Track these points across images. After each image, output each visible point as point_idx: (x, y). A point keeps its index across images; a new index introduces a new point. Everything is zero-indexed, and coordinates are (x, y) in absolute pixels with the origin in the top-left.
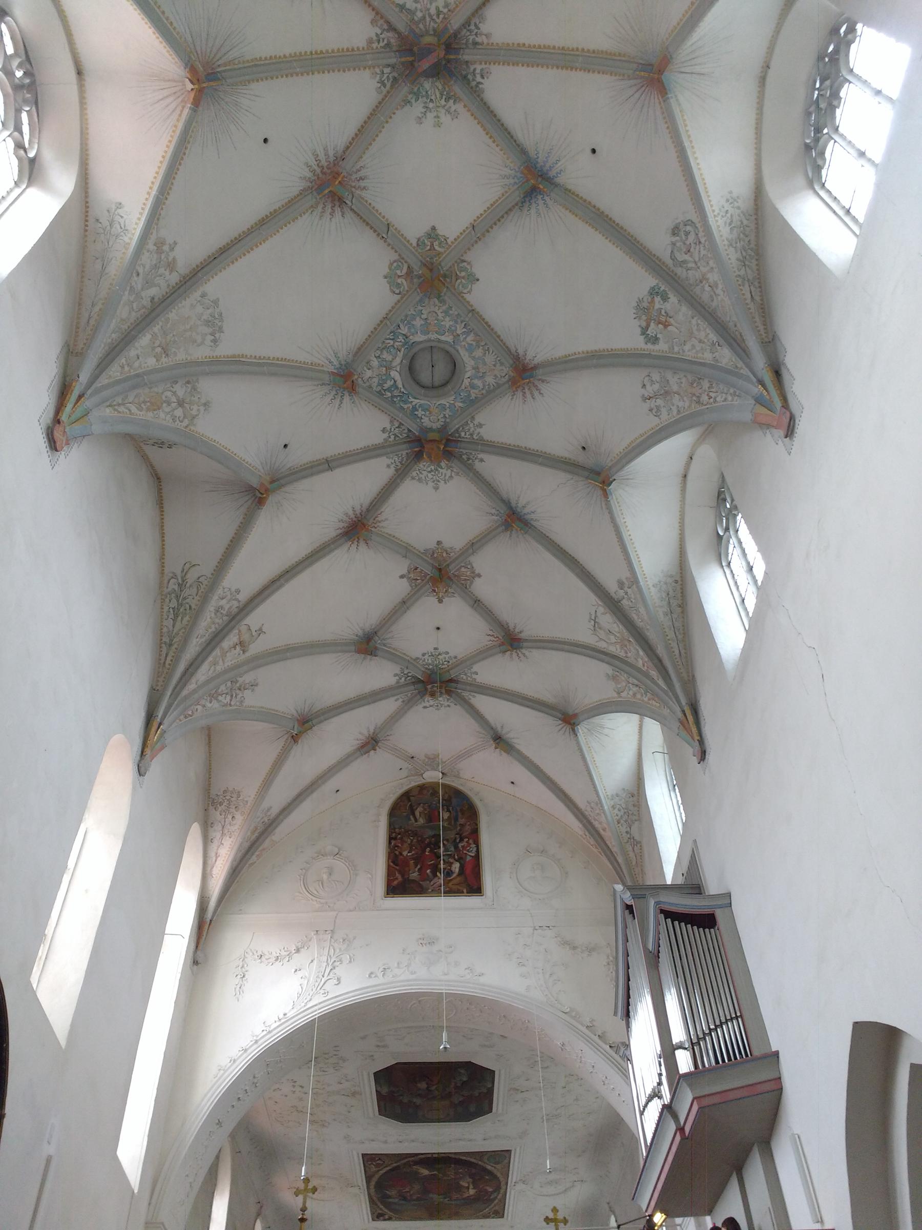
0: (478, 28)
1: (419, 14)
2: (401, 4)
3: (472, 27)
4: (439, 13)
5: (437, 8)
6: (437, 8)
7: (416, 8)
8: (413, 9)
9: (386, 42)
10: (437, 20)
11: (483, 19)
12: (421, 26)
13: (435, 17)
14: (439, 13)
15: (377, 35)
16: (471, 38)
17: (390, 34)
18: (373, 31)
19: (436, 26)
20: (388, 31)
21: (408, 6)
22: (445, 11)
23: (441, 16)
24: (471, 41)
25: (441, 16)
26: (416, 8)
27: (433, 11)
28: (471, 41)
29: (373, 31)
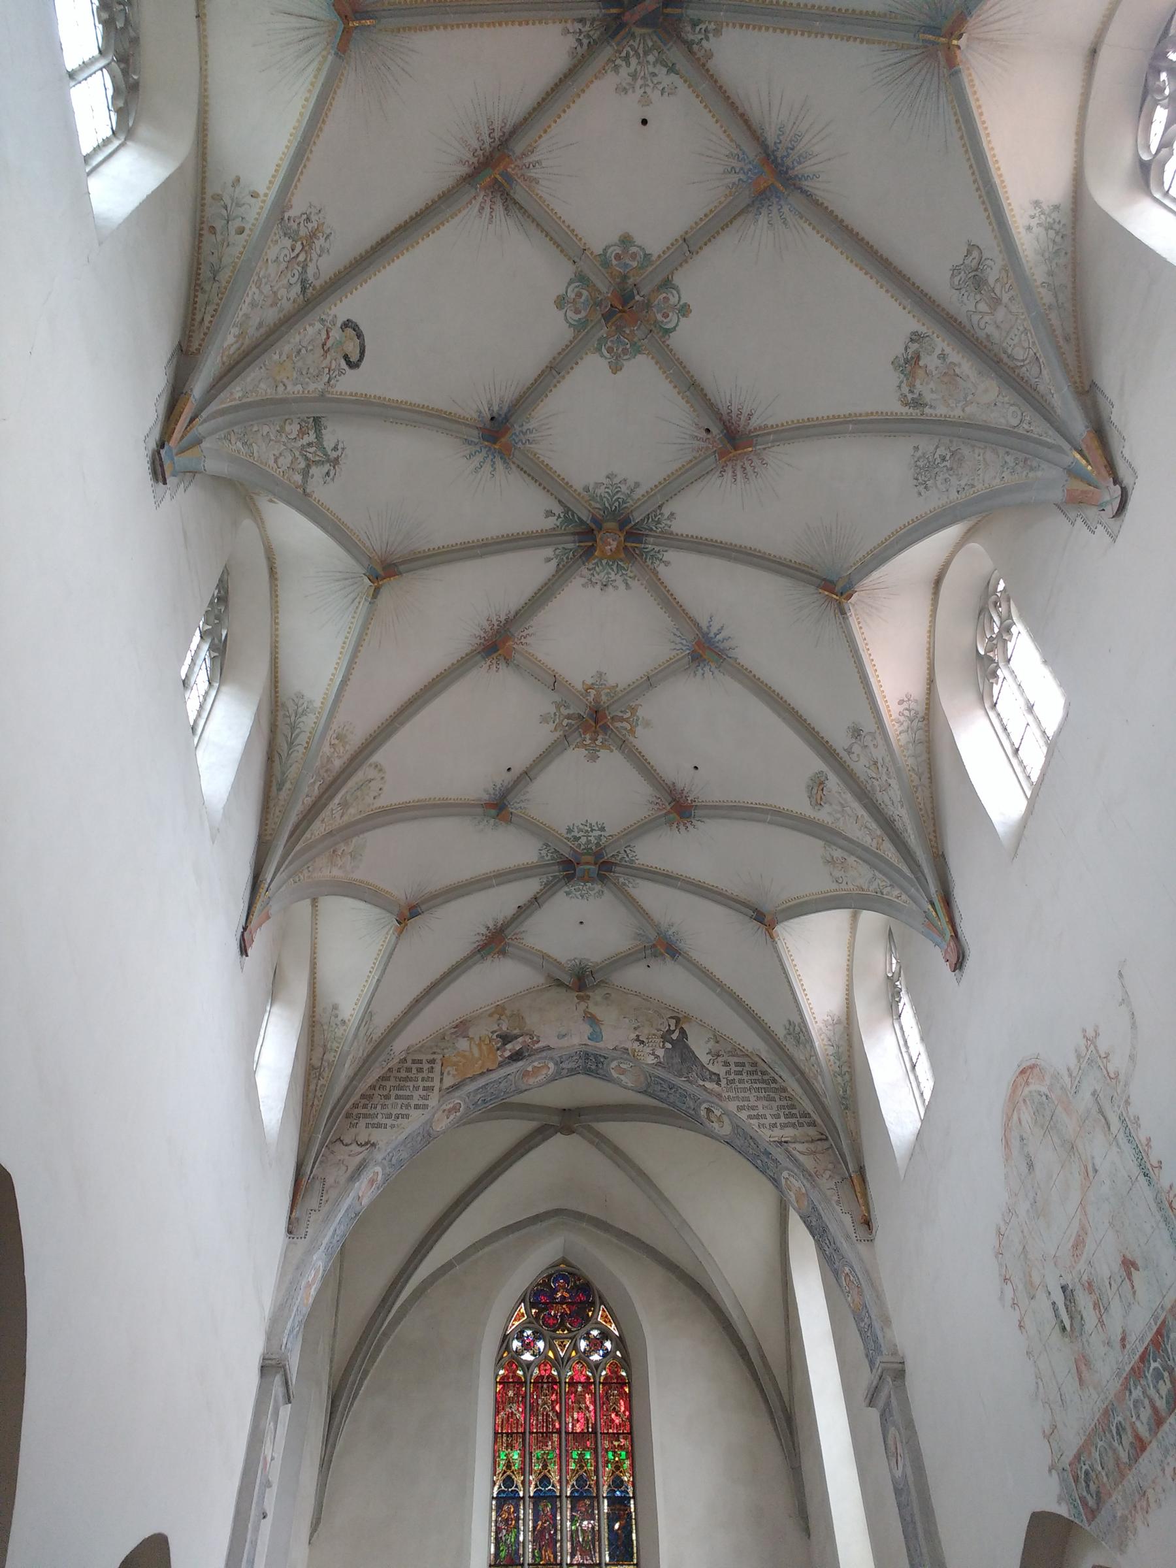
0: (579, 40)
1: (651, 58)
2: (672, 74)
3: (585, 42)
4: (627, 59)
5: (628, 64)
6: (628, 64)
7: (654, 66)
8: (658, 66)
9: (698, 29)
10: (629, 49)
11: (573, 52)
12: (650, 44)
13: (632, 53)
14: (627, 59)
15: (707, 39)
16: (587, 28)
17: (690, 37)
18: (712, 44)
19: (631, 42)
20: (693, 42)
21: (665, 70)
22: (618, 62)
23: (624, 54)
24: (588, 24)
25: (624, 54)
26: (654, 66)
27: (634, 61)
28: (588, 24)
29: (712, 44)
